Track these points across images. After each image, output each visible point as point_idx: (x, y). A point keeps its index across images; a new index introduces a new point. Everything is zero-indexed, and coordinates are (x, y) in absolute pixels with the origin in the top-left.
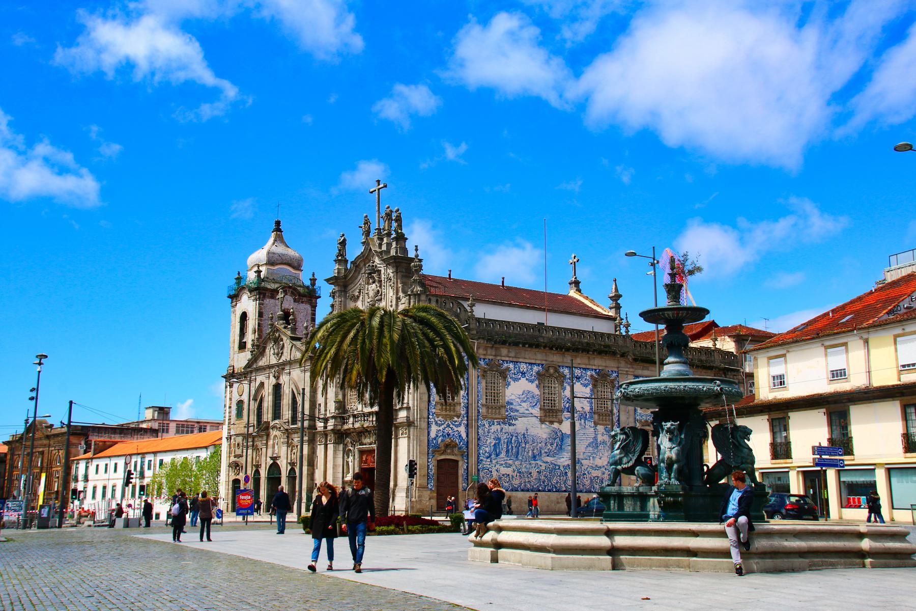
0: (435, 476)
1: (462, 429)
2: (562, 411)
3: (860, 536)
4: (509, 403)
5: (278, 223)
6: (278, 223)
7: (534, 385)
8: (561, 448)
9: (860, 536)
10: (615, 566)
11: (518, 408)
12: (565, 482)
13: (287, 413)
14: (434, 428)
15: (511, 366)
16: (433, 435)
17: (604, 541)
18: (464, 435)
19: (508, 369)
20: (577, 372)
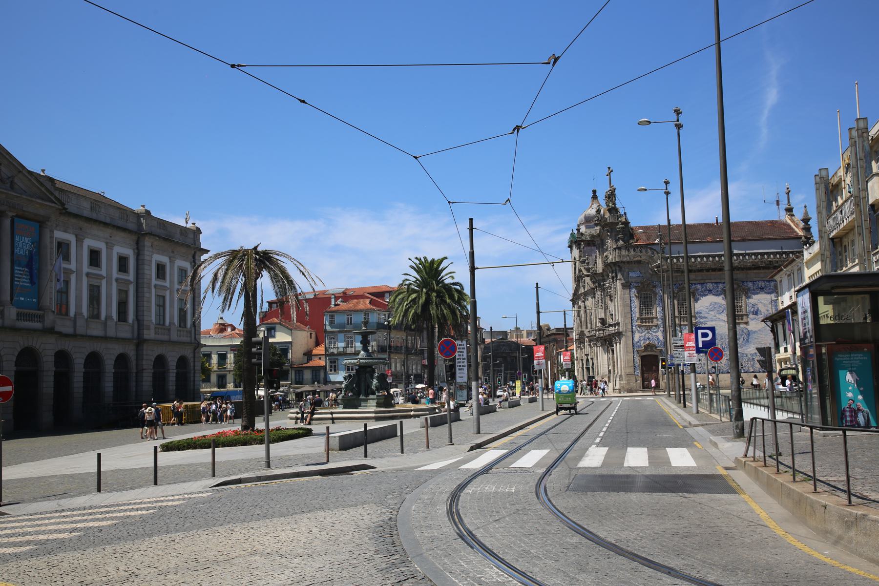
0: (640, 367)
1: (660, 335)
2: (747, 315)
3: (411, 411)
4: (698, 313)
5: (594, 192)
6: (594, 192)
7: (721, 297)
8: (748, 341)
9: (411, 411)
10: (333, 423)
11: (706, 315)
12: (753, 366)
13: (589, 326)
14: (637, 336)
15: (699, 286)
16: (636, 339)
17: (330, 416)
18: (661, 338)
19: (697, 290)
20: (761, 284)
